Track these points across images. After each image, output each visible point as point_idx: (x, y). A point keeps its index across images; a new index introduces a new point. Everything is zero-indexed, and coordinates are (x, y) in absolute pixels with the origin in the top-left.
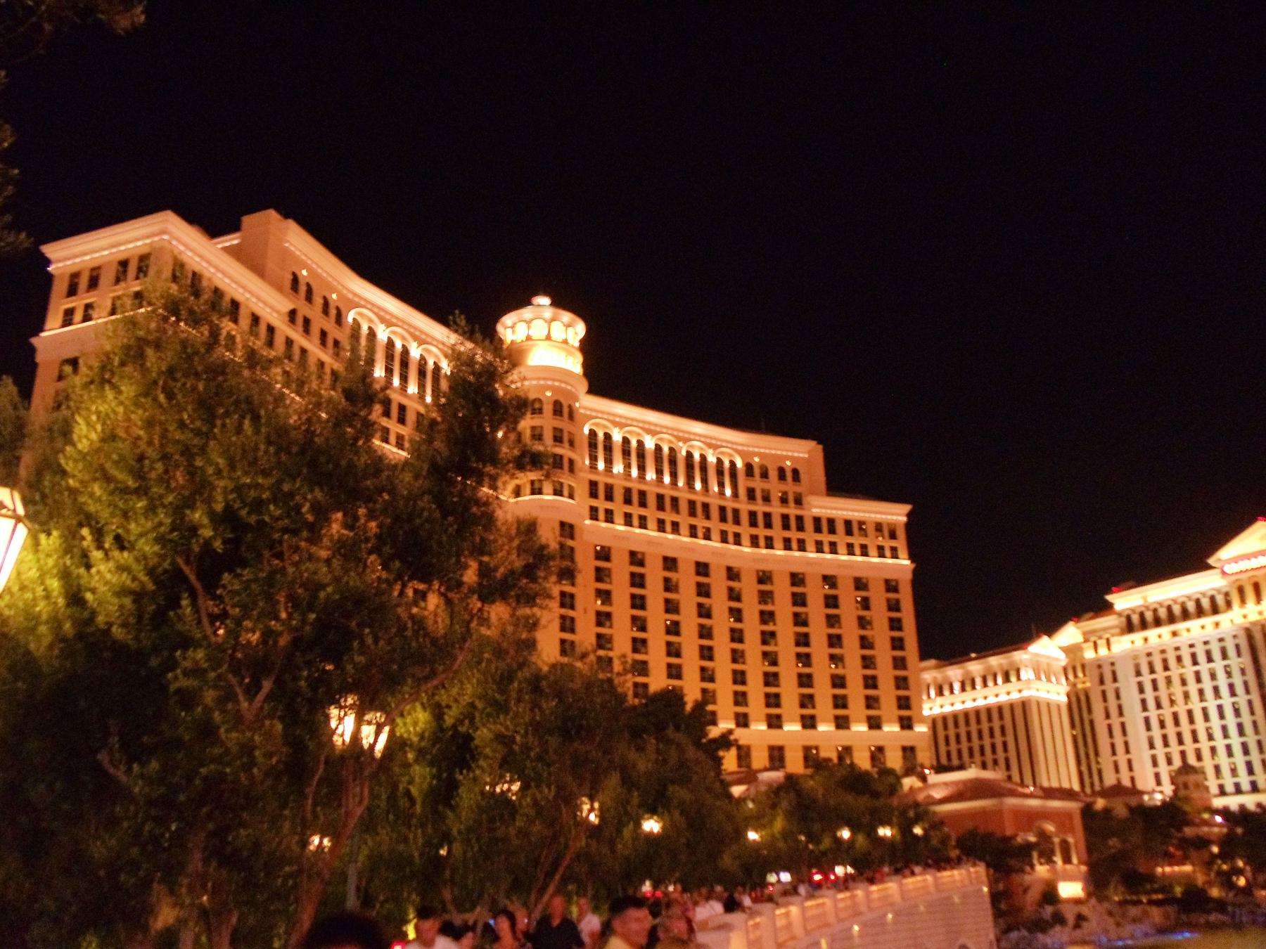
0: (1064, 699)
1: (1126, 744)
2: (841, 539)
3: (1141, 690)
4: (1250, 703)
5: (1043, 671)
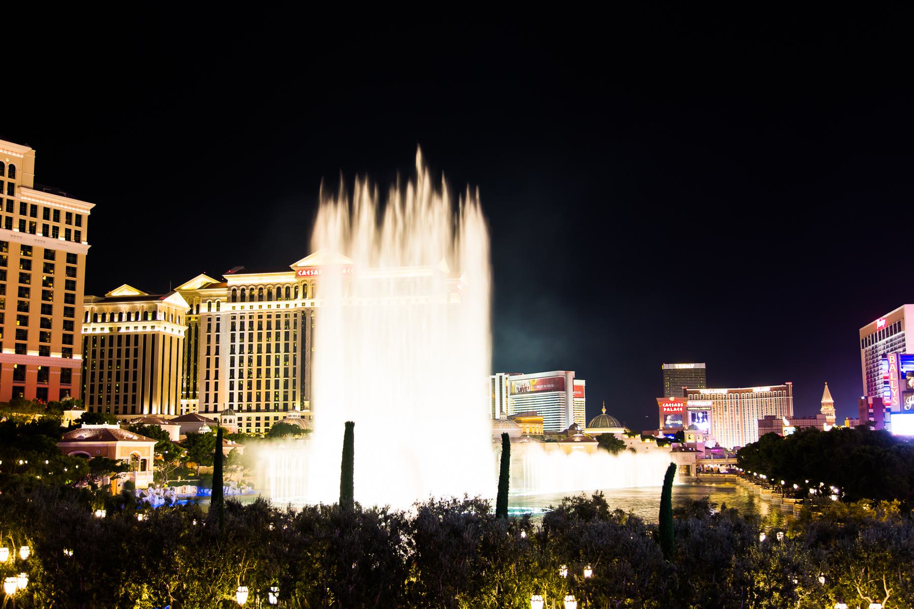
0: (182, 335)
1: (217, 372)
2: (40, 221)
5: (170, 317)
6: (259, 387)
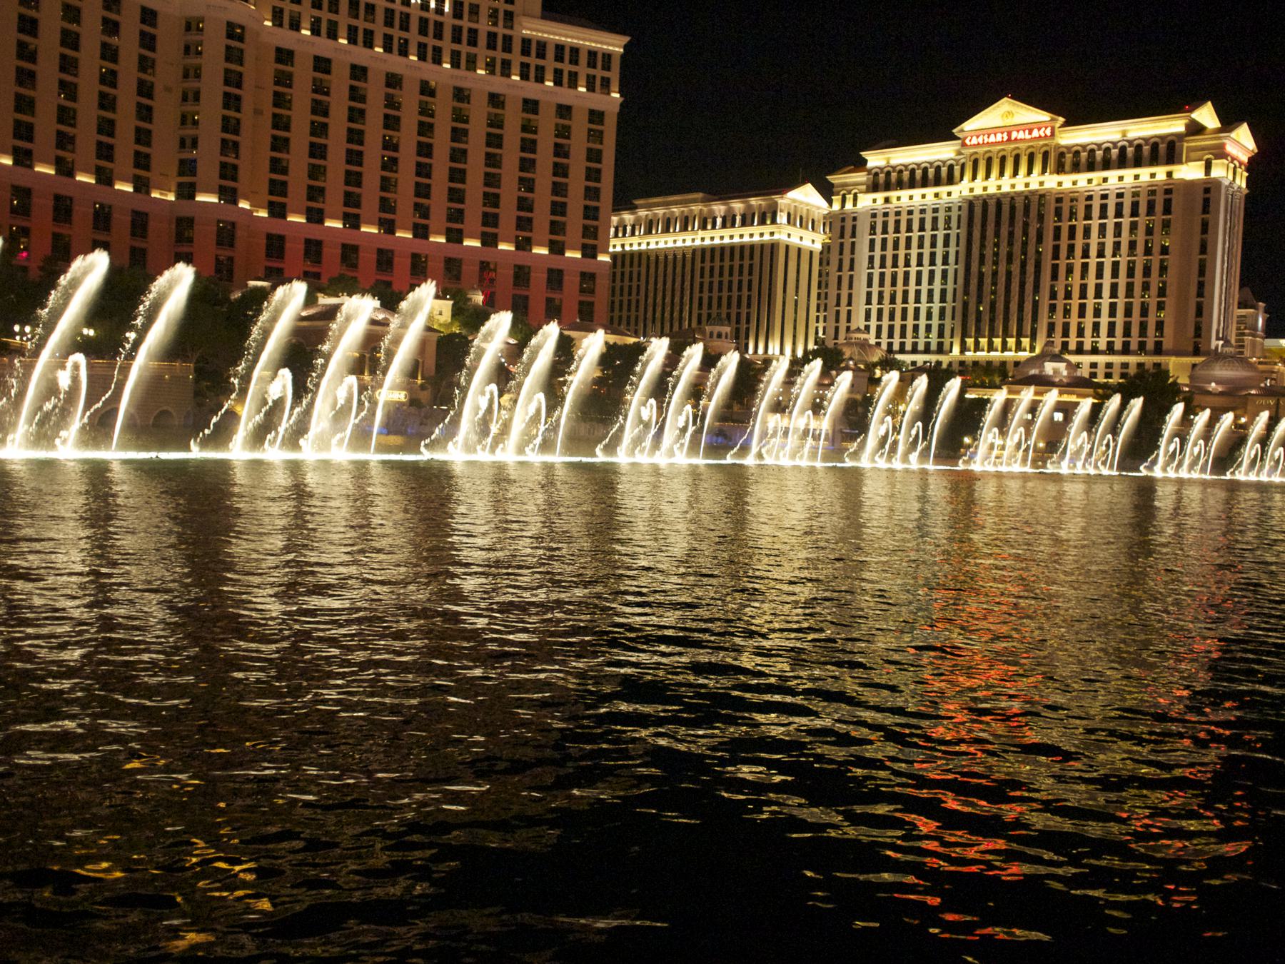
0: (818, 247)
1: (850, 296)
2: (550, 64)
3: (872, 248)
4: (956, 271)
5: (799, 219)
6: (892, 317)
